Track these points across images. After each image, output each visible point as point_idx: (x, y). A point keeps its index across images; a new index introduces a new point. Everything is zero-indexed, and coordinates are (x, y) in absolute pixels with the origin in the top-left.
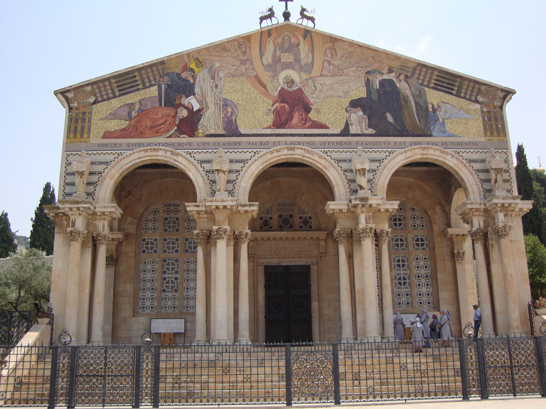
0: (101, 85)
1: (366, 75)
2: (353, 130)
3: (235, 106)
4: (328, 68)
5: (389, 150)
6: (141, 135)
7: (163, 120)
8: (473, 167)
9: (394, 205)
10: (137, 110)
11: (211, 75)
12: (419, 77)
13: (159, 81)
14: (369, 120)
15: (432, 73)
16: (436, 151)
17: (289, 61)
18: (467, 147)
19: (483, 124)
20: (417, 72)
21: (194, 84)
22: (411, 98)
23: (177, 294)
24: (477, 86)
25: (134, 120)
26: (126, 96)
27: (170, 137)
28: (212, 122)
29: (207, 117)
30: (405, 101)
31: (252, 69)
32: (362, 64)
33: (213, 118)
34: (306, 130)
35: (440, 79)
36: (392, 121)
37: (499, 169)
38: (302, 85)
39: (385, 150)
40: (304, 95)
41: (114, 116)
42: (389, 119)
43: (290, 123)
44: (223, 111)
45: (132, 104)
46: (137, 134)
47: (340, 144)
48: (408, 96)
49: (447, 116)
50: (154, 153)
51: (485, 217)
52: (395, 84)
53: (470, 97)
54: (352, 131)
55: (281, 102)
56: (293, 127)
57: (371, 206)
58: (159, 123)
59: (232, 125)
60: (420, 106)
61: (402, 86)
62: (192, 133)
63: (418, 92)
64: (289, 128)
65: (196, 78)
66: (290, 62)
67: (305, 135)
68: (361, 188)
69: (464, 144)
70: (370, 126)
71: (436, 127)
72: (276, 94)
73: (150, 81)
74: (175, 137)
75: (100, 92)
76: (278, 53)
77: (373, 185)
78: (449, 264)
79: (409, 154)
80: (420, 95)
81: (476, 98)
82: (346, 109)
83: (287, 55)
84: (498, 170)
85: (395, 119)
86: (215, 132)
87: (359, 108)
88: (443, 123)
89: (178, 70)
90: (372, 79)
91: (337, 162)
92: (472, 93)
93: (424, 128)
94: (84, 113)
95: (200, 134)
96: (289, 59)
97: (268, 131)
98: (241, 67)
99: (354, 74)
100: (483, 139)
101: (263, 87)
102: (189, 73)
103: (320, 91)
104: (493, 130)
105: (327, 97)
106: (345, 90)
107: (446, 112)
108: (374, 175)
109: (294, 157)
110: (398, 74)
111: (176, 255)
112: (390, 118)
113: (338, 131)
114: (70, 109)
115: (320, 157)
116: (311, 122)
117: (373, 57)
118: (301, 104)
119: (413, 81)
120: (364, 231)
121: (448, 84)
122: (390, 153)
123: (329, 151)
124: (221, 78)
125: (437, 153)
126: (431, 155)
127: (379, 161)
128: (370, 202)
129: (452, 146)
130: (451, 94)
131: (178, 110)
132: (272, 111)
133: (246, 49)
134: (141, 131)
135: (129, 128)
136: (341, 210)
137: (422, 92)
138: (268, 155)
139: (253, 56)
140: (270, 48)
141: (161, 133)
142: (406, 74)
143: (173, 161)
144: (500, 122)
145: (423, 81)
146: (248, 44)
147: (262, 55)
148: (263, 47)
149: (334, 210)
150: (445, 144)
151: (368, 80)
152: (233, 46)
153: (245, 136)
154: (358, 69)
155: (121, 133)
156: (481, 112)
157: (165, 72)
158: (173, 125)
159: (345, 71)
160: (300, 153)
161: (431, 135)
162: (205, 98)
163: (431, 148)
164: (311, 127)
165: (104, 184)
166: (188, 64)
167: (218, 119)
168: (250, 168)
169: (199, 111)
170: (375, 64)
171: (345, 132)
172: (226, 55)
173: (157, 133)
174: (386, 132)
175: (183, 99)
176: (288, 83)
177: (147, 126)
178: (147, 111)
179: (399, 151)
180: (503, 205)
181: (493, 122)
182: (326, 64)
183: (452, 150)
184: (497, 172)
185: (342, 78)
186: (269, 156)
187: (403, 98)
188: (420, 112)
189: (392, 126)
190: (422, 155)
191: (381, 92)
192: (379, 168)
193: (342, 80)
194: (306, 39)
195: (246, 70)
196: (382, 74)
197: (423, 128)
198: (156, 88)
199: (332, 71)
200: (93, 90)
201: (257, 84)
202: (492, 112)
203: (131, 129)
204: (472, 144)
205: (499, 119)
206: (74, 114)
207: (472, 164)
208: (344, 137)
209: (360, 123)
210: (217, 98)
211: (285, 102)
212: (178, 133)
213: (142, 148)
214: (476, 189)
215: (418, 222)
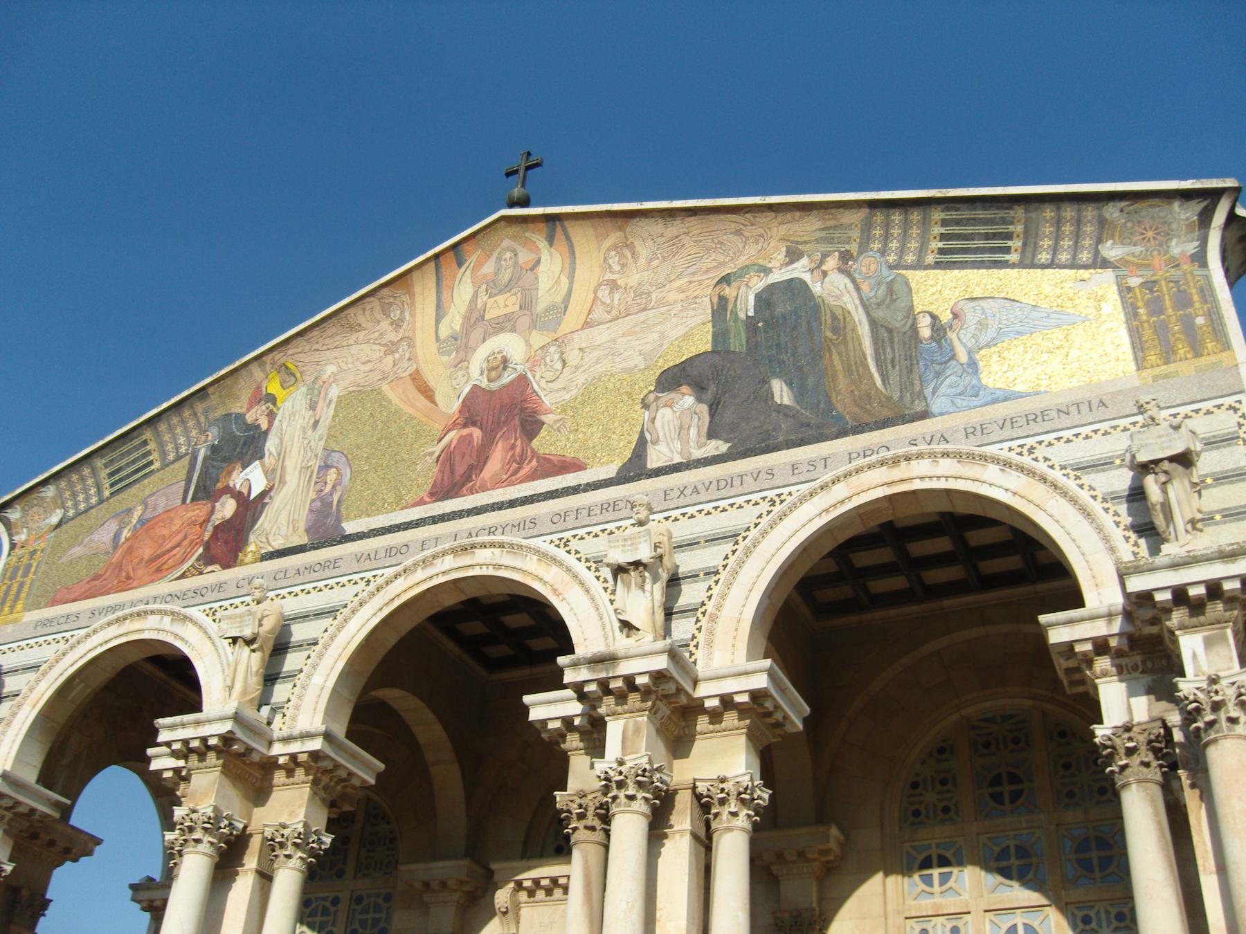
0: (75, 477)
1: (718, 288)
4: (608, 301)
5: (771, 494)
6: (125, 583)
7: (181, 535)
8: (1091, 488)
10: (134, 521)
11: (311, 400)
12: (886, 245)
13: (196, 444)
14: (712, 415)
15: (924, 219)
16: (941, 461)
17: (507, 311)
18: (1065, 421)
19: (1130, 330)
20: (878, 232)
21: (266, 433)
22: (859, 317)
24: (1090, 212)
25: (121, 550)
26: (121, 496)
27: (183, 576)
28: (283, 519)
29: (275, 509)
30: (835, 330)
31: (409, 359)
33: (288, 507)
34: (518, 486)
35: (956, 229)
36: (786, 401)
37: (1172, 459)
38: (528, 365)
39: (755, 497)
40: (529, 391)
42: (777, 399)
43: (477, 476)
44: (316, 483)
45: (130, 510)
46: (119, 582)
47: (611, 509)
48: (846, 313)
49: (984, 339)
50: (137, 624)
51: (1152, 671)
52: (807, 287)
53: (1074, 256)
54: (653, 462)
55: (465, 425)
56: (484, 488)
57: (629, 680)
58: (169, 546)
59: (327, 516)
60: (890, 331)
63: (882, 290)
64: (472, 491)
65: (276, 415)
66: (506, 315)
67: (512, 504)
69: (1054, 414)
70: (712, 434)
71: (948, 382)
72: (456, 405)
73: (177, 448)
74: (193, 575)
75: (74, 496)
77: (704, 621)
79: (840, 491)
81: (1097, 252)
82: (643, 400)
83: (501, 299)
84: (1166, 465)
85: (800, 392)
86: (285, 544)
87: (685, 389)
88: (973, 364)
89: (238, 407)
90: (735, 294)
91: (594, 566)
92: (1076, 243)
93: (901, 398)
94: (34, 552)
95: (250, 554)
96: (506, 306)
98: (384, 361)
99: (682, 296)
101: (426, 397)
102: (264, 408)
103: (577, 368)
104: (1172, 339)
105: (595, 378)
106: (649, 347)
107: (982, 326)
108: (710, 588)
109: (471, 573)
110: (818, 256)
112: (781, 392)
113: (610, 471)
114: (13, 546)
116: (535, 460)
117: (738, 233)
118: (517, 418)
121: (987, 236)
122: (773, 502)
123: (574, 536)
124: (330, 401)
125: (947, 466)
126: (922, 478)
127: (733, 536)
128: (625, 668)
129: (1007, 432)
131: (218, 505)
132: (437, 454)
133: (402, 312)
134: (128, 573)
135: (106, 571)
136: (567, 721)
137: (897, 286)
138: (401, 580)
139: (418, 325)
141: (167, 569)
142: (843, 249)
143: (170, 639)
144: (1197, 305)
145: (902, 251)
146: (406, 298)
147: (439, 316)
148: (445, 295)
149: (544, 722)
150: (978, 433)
151: (723, 300)
152: (367, 313)
153: (353, 540)
154: (697, 278)
155: (88, 586)
156: (1120, 292)
157: (211, 417)
158: (196, 545)
159: (654, 295)
160: (488, 561)
161: (924, 415)
162: (283, 461)
163: (920, 456)
164: (533, 476)
165: (14, 722)
166: (264, 385)
167: (297, 511)
168: (345, 629)
169: (263, 494)
170: (746, 251)
171: (635, 469)
172: (351, 342)
174: (764, 440)
175: (235, 474)
176: (491, 369)
177: (142, 559)
178: (152, 522)
179: (805, 488)
180: (1180, 595)
181: (1170, 311)
182: (604, 293)
183: (1006, 445)
184: (1166, 472)
185: (643, 316)
186: (400, 584)
187: (829, 321)
188: (889, 350)
189: (786, 415)
190: (889, 484)
191: (760, 324)
192: (732, 559)
193: (643, 322)
194: (555, 242)
195: (395, 365)
196: (767, 271)
197: (896, 396)
199: (619, 305)
200: (60, 493)
201: (413, 392)
202: (1163, 283)
203: (108, 573)
204: (1084, 408)
205: (1196, 298)
206: (14, 559)
207: (1087, 479)
208: (627, 485)
209: (682, 430)
210: (309, 454)
211: (474, 424)
212: (201, 563)
213: (111, 617)
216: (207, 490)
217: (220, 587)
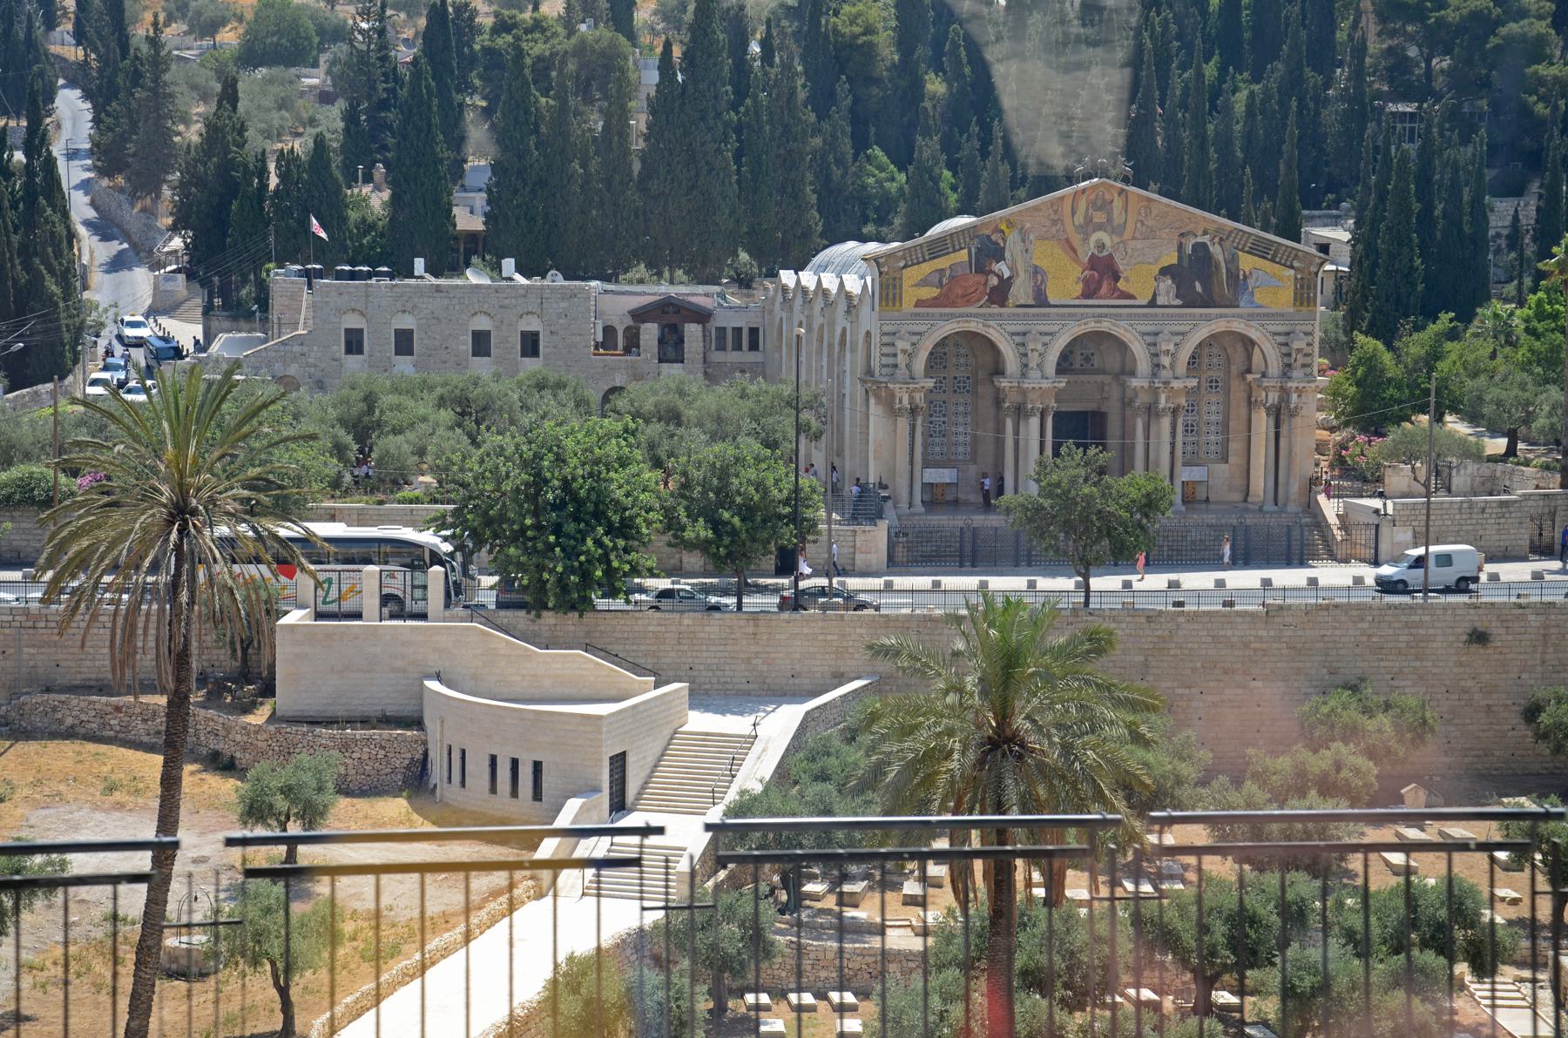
2: (1161, 300)
3: (1044, 274)
6: (953, 304)
9: (1193, 383)
22: (1223, 264)
23: (945, 440)
32: (1176, 225)
41: (924, 282)
45: (943, 270)
54: (1159, 303)
55: (1092, 269)
61: (1216, 250)
62: (1002, 303)
67: (1113, 307)
68: (1164, 367)
70: (1177, 297)
72: (1086, 260)
76: (1091, 211)
78: (1244, 411)
80: (1233, 261)
89: (987, 232)
94: (895, 279)
97: (1077, 302)
100: (1292, 310)
111: (944, 397)
112: (1198, 287)
113: (1145, 302)
114: (881, 273)
115: (1126, 330)
119: (1227, 244)
120: (1164, 409)
125: (1242, 325)
130: (1266, 258)
140: (1082, 204)
147: (1073, 213)
161: (1238, 306)
164: (1118, 298)
169: (1010, 278)
171: (1152, 303)
173: (968, 303)
182: (1139, 225)
198: (966, 251)
209: (1168, 293)
214: (1275, 363)
215: (1215, 360)
216: (981, 268)
217: (1000, 315)
